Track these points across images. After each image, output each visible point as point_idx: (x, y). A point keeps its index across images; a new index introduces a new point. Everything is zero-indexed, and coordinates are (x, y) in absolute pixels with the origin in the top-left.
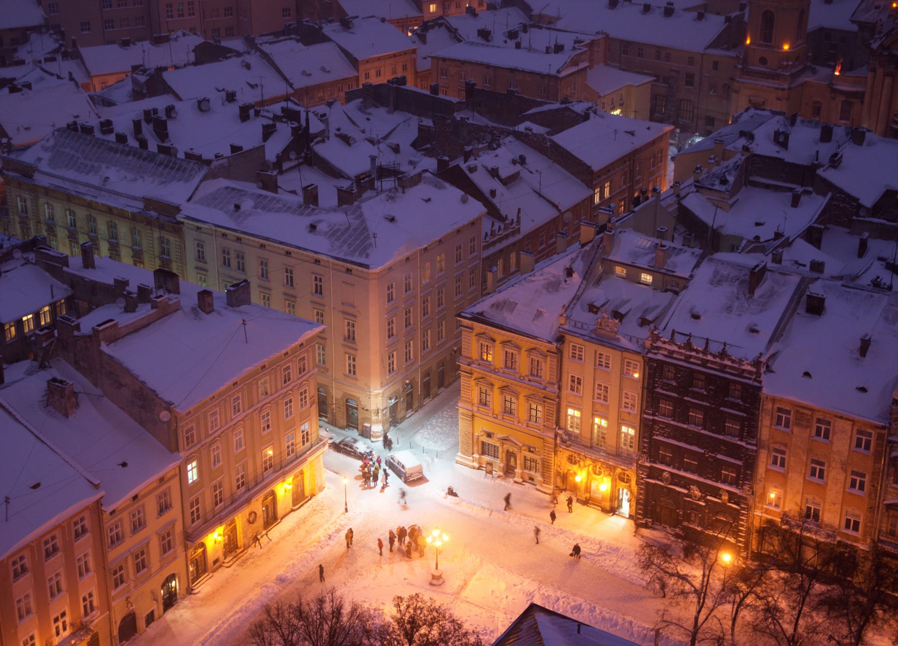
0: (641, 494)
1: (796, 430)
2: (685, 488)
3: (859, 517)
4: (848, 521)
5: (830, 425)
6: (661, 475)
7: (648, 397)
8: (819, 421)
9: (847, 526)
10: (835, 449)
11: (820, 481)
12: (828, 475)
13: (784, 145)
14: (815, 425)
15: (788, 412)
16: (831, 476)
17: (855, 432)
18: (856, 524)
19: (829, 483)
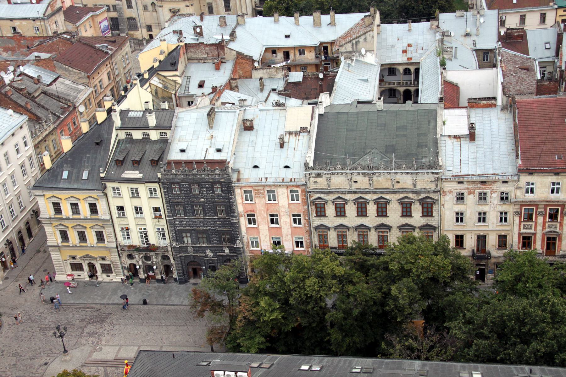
0: (178, 265)
1: (257, 200)
2: (203, 253)
3: (302, 238)
4: (297, 243)
5: (298, 192)
6: (187, 249)
7: (167, 206)
8: (268, 192)
9: (297, 246)
10: (280, 205)
11: (277, 226)
12: (280, 221)
13: (201, 34)
14: (267, 194)
15: (251, 192)
16: (282, 221)
17: (289, 192)
18: (302, 243)
19: (282, 225)
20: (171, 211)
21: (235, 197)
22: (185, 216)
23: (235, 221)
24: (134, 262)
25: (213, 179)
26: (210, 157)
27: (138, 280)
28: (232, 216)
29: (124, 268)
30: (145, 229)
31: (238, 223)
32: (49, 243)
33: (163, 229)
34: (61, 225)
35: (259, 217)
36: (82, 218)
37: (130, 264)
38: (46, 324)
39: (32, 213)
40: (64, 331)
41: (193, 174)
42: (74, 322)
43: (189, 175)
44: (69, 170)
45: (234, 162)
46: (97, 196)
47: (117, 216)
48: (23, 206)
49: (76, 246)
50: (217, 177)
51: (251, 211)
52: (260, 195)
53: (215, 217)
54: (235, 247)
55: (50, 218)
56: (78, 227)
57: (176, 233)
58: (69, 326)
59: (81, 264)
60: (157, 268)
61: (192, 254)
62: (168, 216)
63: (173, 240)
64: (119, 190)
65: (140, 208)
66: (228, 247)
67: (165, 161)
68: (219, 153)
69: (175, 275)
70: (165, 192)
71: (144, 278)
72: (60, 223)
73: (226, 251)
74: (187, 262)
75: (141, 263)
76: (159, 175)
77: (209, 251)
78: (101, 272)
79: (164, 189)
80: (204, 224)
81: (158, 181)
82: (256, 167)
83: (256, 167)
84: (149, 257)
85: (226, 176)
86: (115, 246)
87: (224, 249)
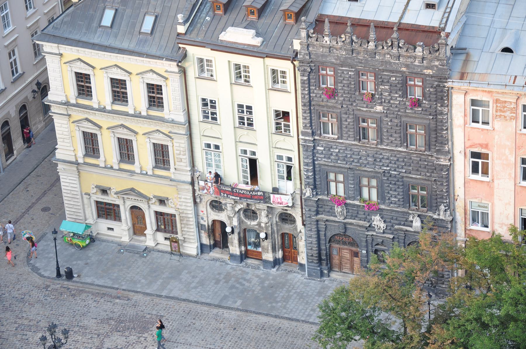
0: (310, 237)
1: (498, 124)
20: (311, 123)
21: (450, 111)
22: (338, 139)
23: (444, 162)
24: (222, 217)
25: (407, 66)
26: (409, 19)
27: (226, 257)
28: (438, 151)
29: (200, 227)
30: (254, 153)
31: (449, 169)
32: (60, 154)
33: (290, 159)
34: (87, 120)
35: (496, 161)
36: (131, 112)
37: (214, 221)
38: (31, 317)
39: (35, 88)
40: (61, 336)
41: (366, 51)
42: (86, 322)
43: (358, 53)
44: (116, 10)
45: (462, 35)
46: (166, 71)
47: (201, 119)
48: (20, 71)
49: (112, 168)
50: (417, 63)
51: (481, 145)
52: (508, 114)
53: (400, 149)
54: (435, 217)
55: (67, 104)
56: (120, 130)
57: (314, 171)
58: (76, 329)
59: (118, 206)
60: (266, 238)
61: (340, 219)
62: (304, 134)
63: (308, 184)
64: (211, 66)
65: (249, 108)
66: (419, 216)
67: (312, 16)
68: (431, 11)
69: (302, 259)
70: (303, 82)
71: (238, 253)
72: (86, 116)
73: (414, 224)
74: (329, 235)
75: (235, 223)
76: (297, 45)
77: (378, 217)
78: (155, 228)
79: (303, 75)
80: (375, 160)
81: (294, 57)
82: (507, 50)
83: (507, 50)
84: (254, 212)
85: (437, 63)
86: (189, 180)
87: (411, 218)
